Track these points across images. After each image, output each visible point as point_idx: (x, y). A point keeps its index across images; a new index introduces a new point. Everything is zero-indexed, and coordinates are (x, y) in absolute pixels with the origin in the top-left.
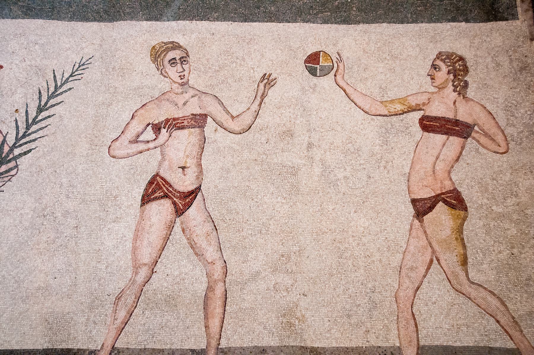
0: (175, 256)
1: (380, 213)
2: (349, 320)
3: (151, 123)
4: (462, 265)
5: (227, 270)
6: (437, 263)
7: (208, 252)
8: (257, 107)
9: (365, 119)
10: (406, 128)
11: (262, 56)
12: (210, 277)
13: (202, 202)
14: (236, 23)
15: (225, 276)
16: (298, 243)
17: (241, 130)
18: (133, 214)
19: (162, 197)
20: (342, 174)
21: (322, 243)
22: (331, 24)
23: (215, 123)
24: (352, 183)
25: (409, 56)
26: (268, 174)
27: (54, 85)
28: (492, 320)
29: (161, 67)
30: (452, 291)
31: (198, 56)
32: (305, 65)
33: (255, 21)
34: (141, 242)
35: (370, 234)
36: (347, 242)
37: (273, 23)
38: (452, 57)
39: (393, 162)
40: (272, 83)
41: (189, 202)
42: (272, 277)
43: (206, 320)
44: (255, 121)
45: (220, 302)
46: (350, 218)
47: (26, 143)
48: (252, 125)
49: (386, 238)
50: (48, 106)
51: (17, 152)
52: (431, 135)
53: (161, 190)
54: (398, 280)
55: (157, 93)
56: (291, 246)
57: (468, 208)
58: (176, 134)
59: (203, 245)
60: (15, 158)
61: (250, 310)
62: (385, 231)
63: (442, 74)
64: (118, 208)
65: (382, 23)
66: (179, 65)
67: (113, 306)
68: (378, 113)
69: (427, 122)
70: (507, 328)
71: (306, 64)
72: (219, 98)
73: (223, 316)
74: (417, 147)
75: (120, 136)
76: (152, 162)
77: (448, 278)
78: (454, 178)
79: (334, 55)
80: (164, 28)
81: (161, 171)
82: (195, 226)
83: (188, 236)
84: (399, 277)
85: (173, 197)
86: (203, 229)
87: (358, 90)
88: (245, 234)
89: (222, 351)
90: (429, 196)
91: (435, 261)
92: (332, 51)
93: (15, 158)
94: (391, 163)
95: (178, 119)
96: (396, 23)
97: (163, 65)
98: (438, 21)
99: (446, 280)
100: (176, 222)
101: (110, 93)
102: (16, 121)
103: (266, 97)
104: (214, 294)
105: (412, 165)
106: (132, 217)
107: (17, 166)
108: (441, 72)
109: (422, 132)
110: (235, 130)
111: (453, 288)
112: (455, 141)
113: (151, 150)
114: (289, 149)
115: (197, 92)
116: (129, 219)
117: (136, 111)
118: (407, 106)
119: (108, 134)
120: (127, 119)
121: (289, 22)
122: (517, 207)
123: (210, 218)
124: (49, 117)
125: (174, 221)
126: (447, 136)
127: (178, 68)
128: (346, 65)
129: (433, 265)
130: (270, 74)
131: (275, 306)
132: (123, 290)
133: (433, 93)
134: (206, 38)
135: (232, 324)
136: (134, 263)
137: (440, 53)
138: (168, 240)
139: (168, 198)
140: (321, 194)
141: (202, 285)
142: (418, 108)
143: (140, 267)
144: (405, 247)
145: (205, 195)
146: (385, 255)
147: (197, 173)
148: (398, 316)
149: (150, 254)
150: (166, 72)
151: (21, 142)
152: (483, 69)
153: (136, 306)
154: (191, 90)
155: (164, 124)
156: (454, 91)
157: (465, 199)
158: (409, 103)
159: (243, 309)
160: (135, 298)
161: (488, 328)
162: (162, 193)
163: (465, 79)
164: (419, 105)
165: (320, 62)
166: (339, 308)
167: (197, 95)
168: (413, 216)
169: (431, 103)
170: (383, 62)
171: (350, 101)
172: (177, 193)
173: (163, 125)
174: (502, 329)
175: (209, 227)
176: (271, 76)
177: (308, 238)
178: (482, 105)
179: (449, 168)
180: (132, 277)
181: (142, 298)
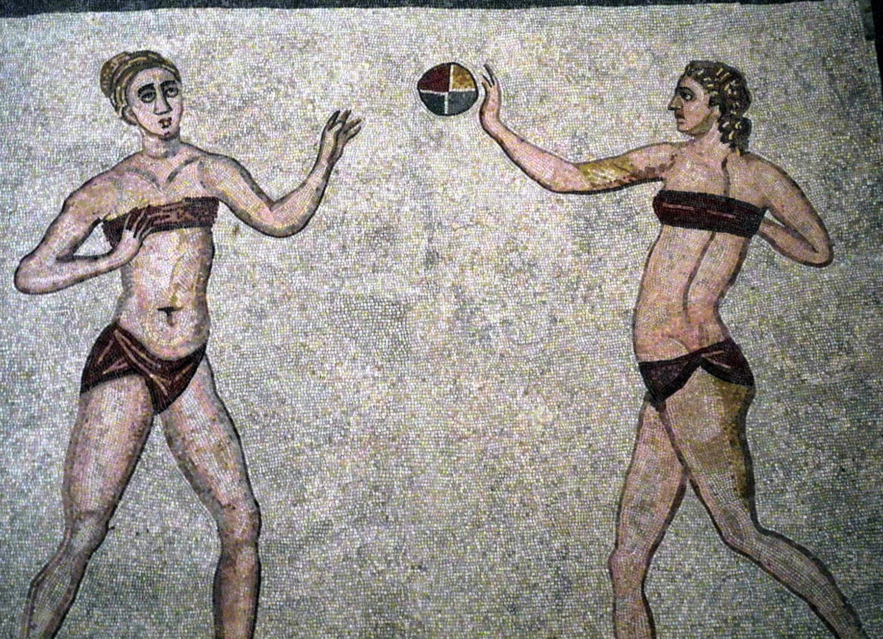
0: (153, 493)
1: (576, 393)
2: (514, 617)
3: (101, 218)
4: (743, 496)
5: (260, 521)
6: (694, 493)
7: (222, 485)
8: (321, 181)
9: (543, 201)
10: (628, 217)
11: (331, 75)
12: (227, 536)
13: (208, 381)
14: (277, 10)
15: (256, 534)
16: (408, 460)
17: (288, 228)
18: (66, 409)
20: (498, 314)
21: (458, 459)
22: (472, 8)
23: (233, 215)
24: (518, 333)
25: (630, 70)
26: (345, 319)
28: (802, 604)
29: (122, 103)
30: (724, 551)
31: (198, 79)
32: (420, 93)
34: (82, 466)
35: (556, 438)
36: (510, 455)
37: (353, 9)
38: (717, 71)
39: (603, 287)
40: (352, 130)
41: (181, 380)
42: (356, 533)
43: (218, 625)
44: (316, 209)
45: (246, 589)
46: (515, 406)
48: (310, 218)
49: (590, 445)
52: (679, 230)
53: (123, 358)
54: (614, 532)
55: (114, 157)
56: (395, 468)
57: (755, 378)
58: (153, 240)
59: (210, 470)
61: (309, 604)
62: (588, 432)
64: (34, 396)
65: (575, 5)
67: (26, 599)
69: (671, 203)
70: (832, 620)
71: (421, 91)
72: (242, 163)
73: (253, 617)
74: (649, 256)
75: (38, 247)
76: (105, 300)
77: (715, 524)
78: (725, 317)
79: (479, 71)
80: (128, 23)
81: (122, 317)
82: (192, 431)
83: (180, 453)
84: (617, 526)
85: (146, 370)
86: (211, 437)
87: (529, 141)
88: (299, 445)
90: (676, 355)
91: (690, 490)
92: (475, 63)
94: (598, 291)
95: (157, 209)
96: (603, 5)
97: (126, 99)
99: (712, 528)
100: (154, 422)
101: (19, 161)
103: (339, 160)
104: (235, 571)
105: (640, 293)
106: (64, 415)
108: (697, 103)
109: (660, 225)
110: (275, 229)
111: (726, 543)
112: (726, 242)
113: (101, 276)
114: (388, 266)
115: (197, 154)
116: (57, 420)
117: (71, 196)
118: (628, 172)
119: (14, 244)
120: (52, 213)
121: (386, 6)
122: (851, 375)
123: (225, 413)
125: (149, 421)
126: (711, 233)
127: (158, 104)
128: (502, 91)
129: (685, 497)
130: (346, 111)
131: (362, 593)
132: (46, 567)
133: (681, 145)
134: (215, 41)
135: (272, 633)
136: (68, 511)
137: (693, 64)
138: (137, 461)
139: (138, 373)
140: (454, 357)
141: (209, 554)
142: (650, 176)
143: (80, 519)
144: (629, 463)
145: (215, 366)
146: (587, 480)
147: (198, 319)
148: (614, 605)
149: (101, 490)
150: (133, 114)
152: (778, 97)
153: (74, 598)
154: (184, 149)
155: (129, 221)
156: (723, 140)
157: (748, 361)
158: (632, 165)
159: (294, 600)
160: (72, 583)
161: (795, 621)
162: (126, 364)
163: (744, 116)
164: (653, 170)
165: (451, 86)
166: (494, 593)
167: (196, 158)
168: (645, 400)
169: (677, 166)
170: (577, 82)
171: (512, 163)
172: (156, 362)
173: (127, 222)
174: (821, 623)
175: (221, 432)
176: (350, 116)
177: (430, 450)
178: (778, 169)
179: (715, 298)
180: (65, 538)
181: (86, 581)
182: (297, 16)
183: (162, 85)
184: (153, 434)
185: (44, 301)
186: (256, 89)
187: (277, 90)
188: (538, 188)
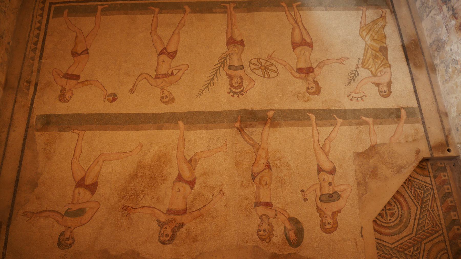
19: (171, 53)
33: (134, 113)
50: (210, 80)
51: (219, 65)
52: (77, 74)
60: (219, 63)
63: (68, 95)
66: (164, 96)
68: (94, 81)
78: (73, 61)
90: (83, 55)
93: (219, 63)
98: (65, 115)
102: (220, 75)
107: (218, 61)
112: (70, 73)
115: (158, 86)
121: (122, 113)
124: (209, 77)
133: (73, 88)
137: (67, 102)
145: (156, 54)
150: (169, 93)
151: (218, 68)
156: (66, 89)
163: (61, 93)
164: (79, 84)
183: (163, 98)
184: (166, 44)
185: (184, 63)
186: (147, 98)
187: (143, 98)
188: (99, 81)
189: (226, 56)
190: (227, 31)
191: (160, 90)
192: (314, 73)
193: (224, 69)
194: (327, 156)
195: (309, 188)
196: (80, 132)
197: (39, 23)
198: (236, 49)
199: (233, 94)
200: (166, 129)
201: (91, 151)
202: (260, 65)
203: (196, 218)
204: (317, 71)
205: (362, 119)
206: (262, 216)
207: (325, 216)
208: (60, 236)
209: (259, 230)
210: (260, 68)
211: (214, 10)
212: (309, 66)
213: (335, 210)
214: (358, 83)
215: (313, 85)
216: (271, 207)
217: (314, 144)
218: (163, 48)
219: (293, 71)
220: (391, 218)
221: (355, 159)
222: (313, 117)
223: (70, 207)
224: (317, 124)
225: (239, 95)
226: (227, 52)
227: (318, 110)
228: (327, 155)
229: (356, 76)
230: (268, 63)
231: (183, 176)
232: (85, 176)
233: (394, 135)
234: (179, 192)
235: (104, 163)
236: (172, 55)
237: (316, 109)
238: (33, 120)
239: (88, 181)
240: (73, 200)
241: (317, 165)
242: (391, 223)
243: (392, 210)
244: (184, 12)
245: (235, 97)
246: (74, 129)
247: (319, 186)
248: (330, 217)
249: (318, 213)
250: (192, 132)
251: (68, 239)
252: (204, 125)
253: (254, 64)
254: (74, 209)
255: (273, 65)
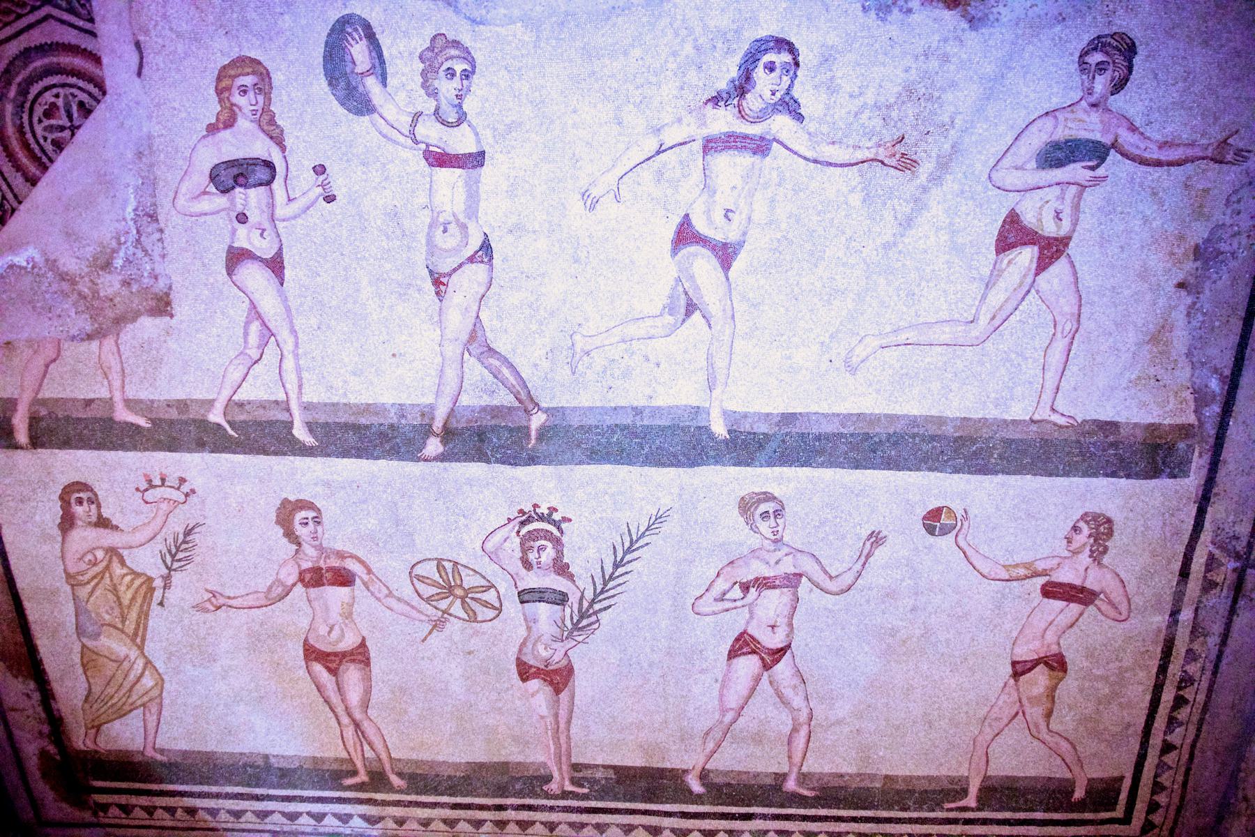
27: (629, 539)
33: (869, 468)
47: (605, 599)
51: (597, 607)
52: (1051, 601)
60: (596, 613)
63: (1082, 539)
89: (803, 774)
93: (596, 613)
95: (769, 578)
98: (1095, 475)
107: (598, 621)
112: (1075, 608)
115: (793, 551)
124: (627, 573)
133: (1065, 558)
137: (1086, 514)
145: (795, 653)
151: (600, 598)
154: (785, 547)
156: (1090, 556)
175: (796, 681)
182: (858, 474)
185: (707, 619)
189: (575, 633)
190: (571, 712)
191: (785, 539)
192: (299, 566)
193: (580, 594)
194: (255, 307)
195: (308, 208)
196: (1047, 418)
197: (1165, 764)
198: (545, 654)
199: (550, 515)
200: (768, 415)
201: (1013, 356)
202: (468, 600)
203: (673, 123)
204: (289, 574)
205: (150, 419)
206: (459, 123)
207: (258, 116)
208: (1127, 80)
209: (467, 75)
210: (467, 591)
211: (611, 774)
212: (313, 592)
213: (225, 134)
214: (164, 530)
215: (301, 531)
216: (431, 148)
217: (297, 345)
218: (775, 668)
219: (366, 577)
220: (53, 100)
221: (167, 295)
222: (300, 432)
223: (1091, 173)
224: (288, 410)
225: (535, 510)
226: (570, 646)
227: (285, 454)
228: (255, 312)
229: (170, 551)
230: (443, 604)
231: (715, 262)
232: (1037, 274)
233: (47, 366)
234: (728, 211)
235: (974, 312)
236: (743, 645)
237: (292, 458)
238: (1198, 464)
239: (1026, 256)
240: (1079, 196)
241: (283, 280)
242: (54, 86)
243: (51, 126)
244: (704, 776)
245: (548, 505)
246: (1067, 427)
247: (279, 212)
248: (240, 110)
249: (278, 127)
250: (684, 403)
251: (1101, 67)
252: (646, 422)
253: (486, 604)
254: (1078, 165)
255: (428, 600)
